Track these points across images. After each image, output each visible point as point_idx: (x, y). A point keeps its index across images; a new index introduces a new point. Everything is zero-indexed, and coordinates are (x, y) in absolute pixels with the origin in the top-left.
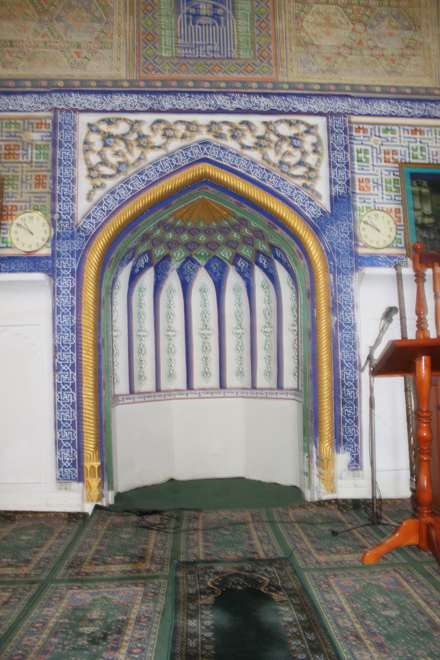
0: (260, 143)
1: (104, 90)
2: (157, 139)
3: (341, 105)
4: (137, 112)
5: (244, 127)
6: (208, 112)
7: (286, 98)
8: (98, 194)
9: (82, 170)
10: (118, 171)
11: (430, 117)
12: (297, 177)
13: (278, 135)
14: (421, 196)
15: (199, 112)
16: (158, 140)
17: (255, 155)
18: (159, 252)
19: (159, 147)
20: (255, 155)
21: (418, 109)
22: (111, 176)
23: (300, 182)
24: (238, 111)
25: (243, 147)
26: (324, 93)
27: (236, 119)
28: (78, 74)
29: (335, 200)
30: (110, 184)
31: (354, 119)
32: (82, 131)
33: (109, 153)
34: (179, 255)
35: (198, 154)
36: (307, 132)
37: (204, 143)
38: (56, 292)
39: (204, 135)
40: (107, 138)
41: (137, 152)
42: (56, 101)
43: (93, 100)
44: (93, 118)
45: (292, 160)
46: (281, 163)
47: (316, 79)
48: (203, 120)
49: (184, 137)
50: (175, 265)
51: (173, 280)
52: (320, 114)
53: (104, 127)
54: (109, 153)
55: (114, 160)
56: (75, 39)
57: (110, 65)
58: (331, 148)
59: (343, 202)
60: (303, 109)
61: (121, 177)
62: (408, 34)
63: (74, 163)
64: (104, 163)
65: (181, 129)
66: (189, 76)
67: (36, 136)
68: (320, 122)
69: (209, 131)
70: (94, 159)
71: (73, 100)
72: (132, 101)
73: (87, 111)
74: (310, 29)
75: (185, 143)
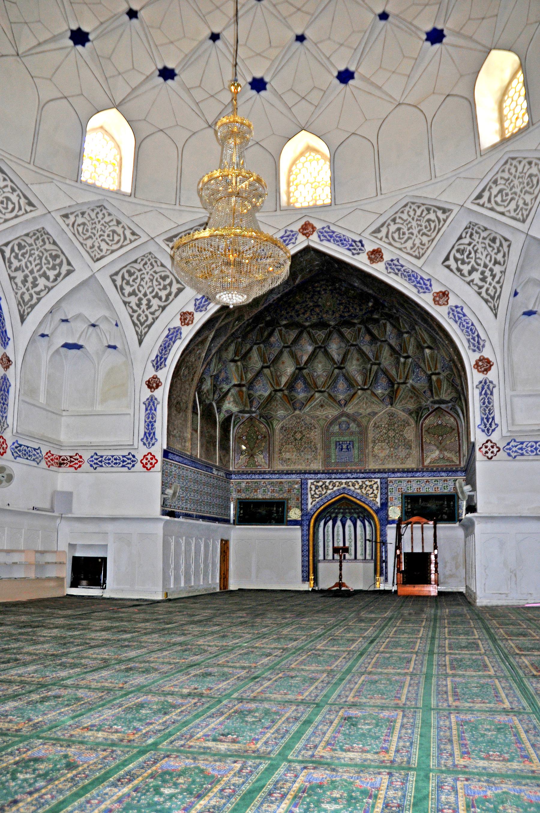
0: (361, 487)
1: (316, 473)
2: (331, 487)
3: (386, 475)
7: (369, 474)
9: (309, 496)
14: (408, 503)
16: (331, 487)
17: (359, 491)
18: (333, 515)
20: (359, 491)
21: (410, 475)
26: (379, 472)
27: (353, 480)
28: (308, 468)
29: (382, 504)
34: (340, 517)
35: (342, 491)
39: (344, 486)
40: (317, 487)
42: (302, 476)
43: (312, 476)
47: (377, 467)
48: (344, 481)
50: (339, 519)
51: (339, 523)
56: (307, 457)
57: (316, 466)
58: (381, 489)
59: (385, 505)
66: (339, 468)
68: (379, 480)
70: (313, 493)
71: (306, 476)
74: (376, 451)
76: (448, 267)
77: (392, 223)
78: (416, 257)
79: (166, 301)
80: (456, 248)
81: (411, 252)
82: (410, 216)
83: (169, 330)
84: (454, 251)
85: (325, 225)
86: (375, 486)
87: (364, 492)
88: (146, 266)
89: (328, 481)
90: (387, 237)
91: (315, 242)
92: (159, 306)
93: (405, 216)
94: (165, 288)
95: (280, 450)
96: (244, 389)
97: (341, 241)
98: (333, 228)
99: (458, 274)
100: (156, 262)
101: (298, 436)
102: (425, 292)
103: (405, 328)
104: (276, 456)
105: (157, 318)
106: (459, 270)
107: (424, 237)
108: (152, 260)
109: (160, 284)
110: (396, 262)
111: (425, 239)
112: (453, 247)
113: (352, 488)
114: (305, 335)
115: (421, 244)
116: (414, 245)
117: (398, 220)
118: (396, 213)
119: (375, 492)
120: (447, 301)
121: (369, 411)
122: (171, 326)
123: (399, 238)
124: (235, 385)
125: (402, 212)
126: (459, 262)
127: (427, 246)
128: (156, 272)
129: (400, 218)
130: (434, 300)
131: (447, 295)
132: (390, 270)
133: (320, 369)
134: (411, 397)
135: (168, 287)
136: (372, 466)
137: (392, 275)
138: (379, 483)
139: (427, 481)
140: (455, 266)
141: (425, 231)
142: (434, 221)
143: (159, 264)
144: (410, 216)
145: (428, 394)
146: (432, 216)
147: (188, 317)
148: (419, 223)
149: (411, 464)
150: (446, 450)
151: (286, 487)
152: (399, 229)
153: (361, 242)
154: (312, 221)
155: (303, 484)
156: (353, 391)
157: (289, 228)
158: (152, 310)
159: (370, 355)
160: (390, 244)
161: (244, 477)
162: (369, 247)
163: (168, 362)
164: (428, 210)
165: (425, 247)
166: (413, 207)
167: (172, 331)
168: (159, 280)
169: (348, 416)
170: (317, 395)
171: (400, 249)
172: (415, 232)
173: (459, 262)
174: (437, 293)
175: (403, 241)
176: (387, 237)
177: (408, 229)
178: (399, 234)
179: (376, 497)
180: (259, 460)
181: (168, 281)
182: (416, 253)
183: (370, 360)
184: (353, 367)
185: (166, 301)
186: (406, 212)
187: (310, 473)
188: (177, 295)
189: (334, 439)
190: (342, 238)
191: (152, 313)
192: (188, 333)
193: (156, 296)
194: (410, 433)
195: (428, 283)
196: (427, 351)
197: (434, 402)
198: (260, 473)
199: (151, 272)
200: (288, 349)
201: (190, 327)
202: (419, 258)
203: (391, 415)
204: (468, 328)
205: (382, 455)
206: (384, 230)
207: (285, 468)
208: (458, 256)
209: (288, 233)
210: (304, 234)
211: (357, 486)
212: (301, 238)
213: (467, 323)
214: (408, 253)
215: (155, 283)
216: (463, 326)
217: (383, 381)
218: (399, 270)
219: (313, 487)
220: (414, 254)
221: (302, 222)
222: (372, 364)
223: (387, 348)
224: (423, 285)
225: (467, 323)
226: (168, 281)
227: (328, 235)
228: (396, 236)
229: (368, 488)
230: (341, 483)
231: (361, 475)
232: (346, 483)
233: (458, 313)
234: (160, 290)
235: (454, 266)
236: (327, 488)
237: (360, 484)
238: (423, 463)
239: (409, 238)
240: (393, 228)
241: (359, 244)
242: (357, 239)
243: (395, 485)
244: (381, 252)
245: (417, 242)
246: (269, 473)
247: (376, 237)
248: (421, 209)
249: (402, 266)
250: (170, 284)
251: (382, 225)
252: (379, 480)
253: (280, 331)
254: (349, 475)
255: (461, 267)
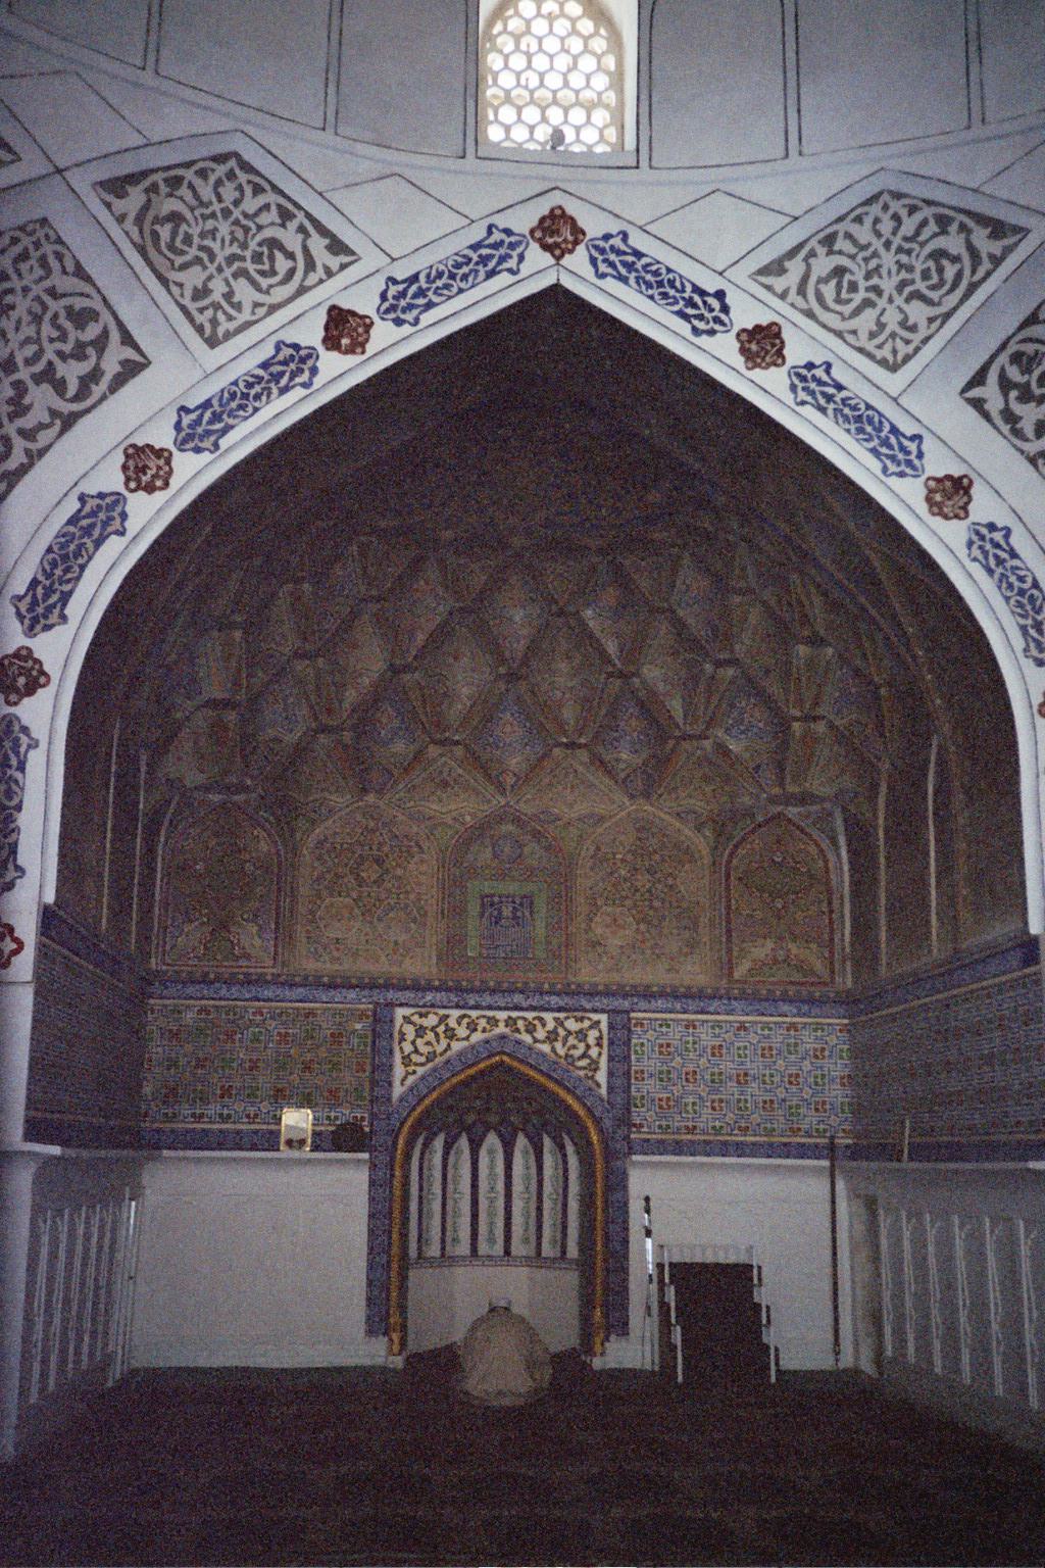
0: (552, 1037)
1: (417, 987)
2: (462, 1032)
4: (445, 1007)
5: (536, 1022)
6: (506, 1009)
7: (575, 997)
8: (411, 1079)
10: (428, 1060)
11: (702, 1012)
12: (581, 1068)
13: (565, 1029)
15: (500, 1008)
16: (462, 1032)
19: (463, 1039)
20: (546, 1048)
21: (692, 1005)
22: (422, 1065)
23: (582, 1073)
24: (533, 1008)
25: (536, 1041)
26: (608, 993)
27: (530, 1015)
30: (420, 1071)
31: (633, 1015)
32: (399, 1021)
33: (419, 1041)
36: (591, 1027)
37: (503, 1037)
38: (373, 1167)
39: (501, 1029)
40: (420, 1031)
41: (444, 1043)
42: (379, 997)
43: (409, 995)
44: (407, 1011)
45: (577, 1053)
46: (567, 1055)
47: (601, 979)
48: (502, 1015)
49: (484, 1031)
52: (603, 1011)
53: (416, 1018)
54: (419, 1041)
55: (424, 1049)
57: (421, 965)
58: (611, 1043)
60: (588, 1006)
61: (430, 1065)
62: (687, 934)
63: (391, 1052)
64: (416, 1051)
65: (483, 1023)
67: (358, 1026)
68: (603, 1018)
69: (507, 1026)
70: (408, 1048)
71: (391, 995)
72: (440, 997)
73: (401, 1005)
74: (599, 931)
75: (486, 1035)
76: (978, 404)
77: (821, 251)
78: (883, 363)
79: (77, 398)
80: (1013, 348)
81: (870, 346)
82: (878, 235)
83: (82, 498)
84: (1003, 359)
85: (614, 227)
86: (593, 1035)
87: (561, 1051)
88: (24, 267)
89: (455, 1013)
90: (802, 291)
91: (578, 275)
92: (54, 413)
93: (863, 234)
94: (79, 353)
95: (312, 912)
96: (231, 717)
97: (661, 284)
98: (638, 241)
99: (1006, 429)
100: (59, 257)
101: (370, 873)
102: (902, 475)
103: (744, 577)
104: (300, 931)
105: (42, 453)
106: (1010, 417)
107: (916, 304)
108: (48, 249)
109: (63, 338)
110: (820, 373)
111: (918, 312)
112: (1003, 346)
113: (528, 1039)
114: (432, 572)
115: (903, 324)
116: (881, 326)
117: (841, 244)
118: (840, 219)
119: (594, 1052)
120: (965, 508)
121: (581, 808)
122: (91, 487)
123: (838, 301)
124: (213, 704)
125: (859, 220)
126: (1013, 394)
127: (923, 332)
128: (52, 292)
129: (849, 236)
130: (928, 499)
131: (967, 491)
132: (802, 395)
133: (466, 679)
134: (706, 779)
135: (90, 351)
136: (588, 973)
137: (808, 411)
138: (604, 1026)
139: (742, 1027)
140: (1001, 405)
141: (921, 286)
142: (956, 259)
143: (70, 267)
144: (878, 235)
145: (768, 775)
146: (953, 243)
147: (153, 463)
148: (904, 259)
149: (695, 972)
150: (795, 939)
151: (327, 1027)
152: (839, 272)
153: (720, 295)
154: (573, 208)
155: (380, 1022)
156: (540, 750)
157: (501, 221)
158: (27, 422)
159: (611, 647)
160: (810, 314)
161: (191, 990)
162: (746, 314)
163: (74, 608)
164: (943, 222)
165: (917, 338)
166: (895, 206)
167: (91, 504)
168: (63, 321)
169: (517, 821)
170: (433, 751)
171: (839, 334)
172: (888, 285)
173: (1013, 394)
174: (938, 480)
175: (847, 309)
176: (802, 291)
177: (868, 276)
178: (839, 286)
179: (594, 1066)
180: (245, 941)
181: (92, 331)
182: (886, 352)
183: (608, 661)
184: (561, 679)
185: (77, 398)
186: (868, 221)
187: (403, 987)
188: (119, 382)
189: (478, 887)
190: (665, 277)
191: (28, 435)
192: (149, 516)
193: (48, 376)
194: (694, 884)
195: (912, 447)
196: (803, 650)
197: (773, 800)
198: (249, 981)
199: (37, 290)
200: (374, 607)
201: (160, 497)
202: (894, 368)
203: (643, 828)
204: (1022, 592)
205: (615, 942)
206: (795, 268)
207: (326, 967)
208: (1014, 373)
209: (497, 236)
210: (546, 247)
211: (541, 1034)
212: (537, 257)
213: (1021, 579)
214: (861, 350)
215: (47, 329)
216: (1010, 586)
217: (631, 724)
218: (829, 398)
219: (410, 1031)
220: (879, 354)
221: (543, 208)
222: (610, 675)
223: (664, 627)
224: (898, 449)
225: (1021, 579)
226: (92, 331)
227: (621, 259)
228: (829, 291)
229: (572, 1041)
230: (493, 1022)
231: (554, 1000)
232: (510, 1022)
233: (997, 546)
234: (60, 354)
235: (995, 404)
236: (451, 1034)
237: (551, 1025)
238: (731, 974)
239: (867, 303)
240: (823, 265)
241: (714, 303)
242: (711, 284)
243: (651, 1034)
244: (778, 335)
245: (892, 319)
246: (276, 981)
247: (769, 288)
248: (918, 217)
249: (840, 387)
250: (101, 343)
251: (792, 253)
252: (603, 1018)
253: (364, 550)
254: (518, 998)
255: (1017, 408)
